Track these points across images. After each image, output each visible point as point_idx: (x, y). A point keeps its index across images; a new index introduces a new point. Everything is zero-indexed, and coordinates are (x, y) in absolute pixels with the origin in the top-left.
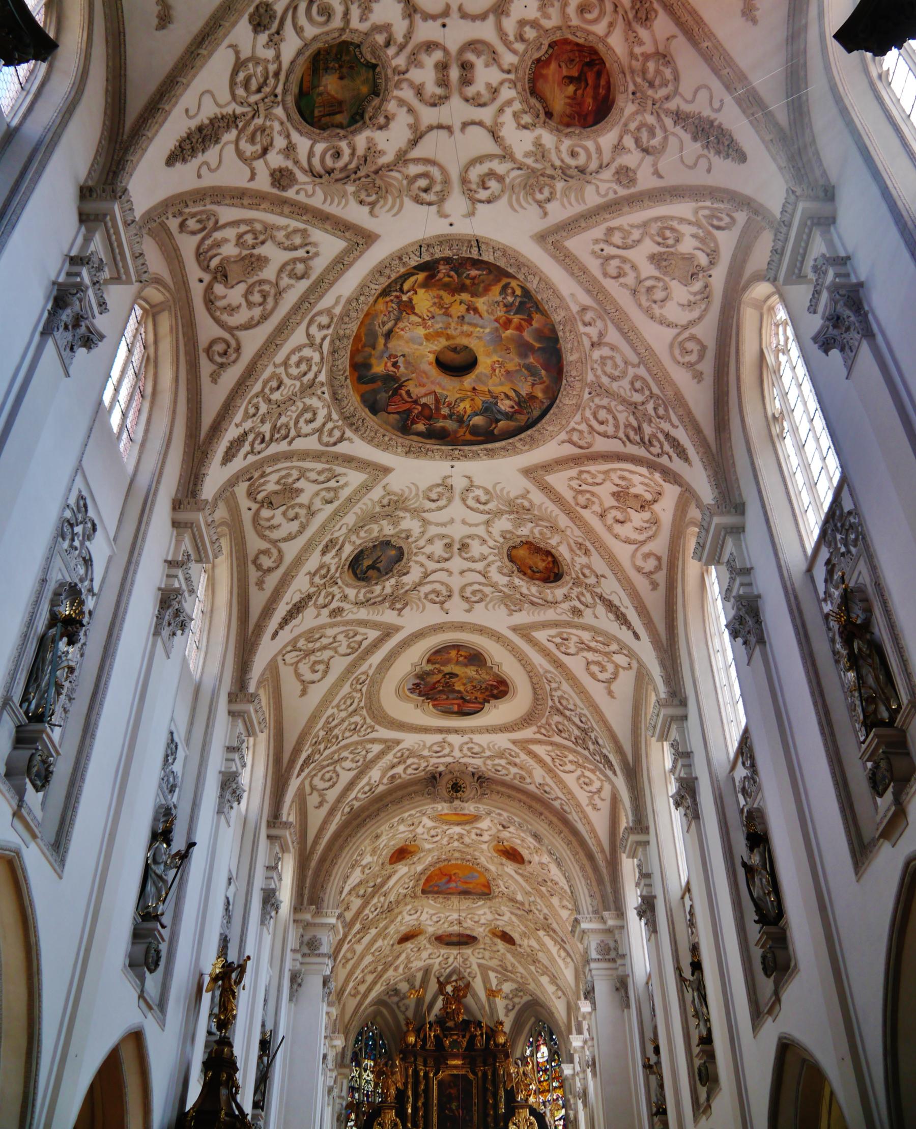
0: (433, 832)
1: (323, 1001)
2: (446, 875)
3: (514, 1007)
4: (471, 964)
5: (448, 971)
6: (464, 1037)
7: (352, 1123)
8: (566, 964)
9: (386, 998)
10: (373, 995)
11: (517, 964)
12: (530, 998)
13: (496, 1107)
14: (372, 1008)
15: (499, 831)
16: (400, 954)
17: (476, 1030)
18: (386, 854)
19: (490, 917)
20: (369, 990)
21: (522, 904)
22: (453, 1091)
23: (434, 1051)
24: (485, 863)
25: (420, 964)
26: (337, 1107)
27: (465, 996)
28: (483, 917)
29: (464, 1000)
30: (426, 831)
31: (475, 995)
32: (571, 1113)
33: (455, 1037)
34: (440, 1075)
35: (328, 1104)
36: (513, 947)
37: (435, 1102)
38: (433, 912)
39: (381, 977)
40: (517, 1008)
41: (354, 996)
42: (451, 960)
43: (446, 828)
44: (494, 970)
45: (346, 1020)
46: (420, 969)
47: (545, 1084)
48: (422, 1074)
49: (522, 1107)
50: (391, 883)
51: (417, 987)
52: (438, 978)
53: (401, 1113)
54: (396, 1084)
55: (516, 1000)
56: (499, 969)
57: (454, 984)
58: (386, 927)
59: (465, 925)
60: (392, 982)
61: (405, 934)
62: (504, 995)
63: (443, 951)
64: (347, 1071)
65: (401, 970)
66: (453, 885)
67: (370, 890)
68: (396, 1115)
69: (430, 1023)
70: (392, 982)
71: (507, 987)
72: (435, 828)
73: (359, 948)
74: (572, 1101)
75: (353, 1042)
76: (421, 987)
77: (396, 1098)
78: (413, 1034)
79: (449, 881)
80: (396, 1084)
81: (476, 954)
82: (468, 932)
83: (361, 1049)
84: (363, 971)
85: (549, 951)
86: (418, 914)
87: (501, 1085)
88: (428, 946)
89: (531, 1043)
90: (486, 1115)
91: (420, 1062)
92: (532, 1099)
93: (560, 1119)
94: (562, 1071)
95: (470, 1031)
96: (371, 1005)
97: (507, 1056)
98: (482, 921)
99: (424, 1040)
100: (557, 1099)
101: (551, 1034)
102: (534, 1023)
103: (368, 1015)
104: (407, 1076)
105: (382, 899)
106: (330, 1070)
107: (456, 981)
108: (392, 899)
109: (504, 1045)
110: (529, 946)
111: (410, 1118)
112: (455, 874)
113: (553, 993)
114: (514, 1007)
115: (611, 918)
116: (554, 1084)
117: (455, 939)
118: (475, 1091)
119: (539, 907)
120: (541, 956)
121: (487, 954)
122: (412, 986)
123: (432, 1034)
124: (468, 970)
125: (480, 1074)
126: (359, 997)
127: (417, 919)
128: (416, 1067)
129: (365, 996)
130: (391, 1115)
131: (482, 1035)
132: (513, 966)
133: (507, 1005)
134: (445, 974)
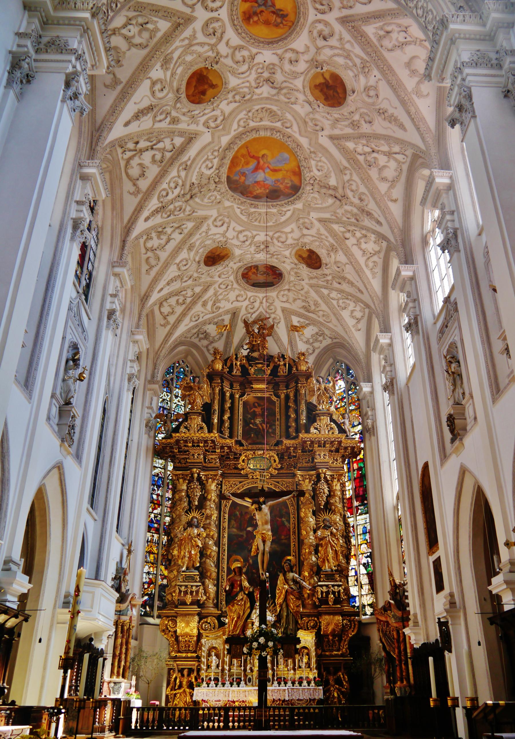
0: (238, 56)
2: (253, 157)
3: (314, 351)
4: (276, 308)
5: (254, 316)
6: (268, 366)
8: (374, 274)
9: (196, 341)
11: (320, 301)
12: (328, 341)
14: (183, 347)
15: (318, 49)
16: (208, 287)
17: (279, 361)
18: (182, 75)
19: (297, 234)
21: (335, 189)
22: (258, 410)
23: (240, 376)
24: (297, 135)
26: (146, 416)
28: (290, 236)
29: (267, 338)
30: (230, 51)
31: (278, 340)
32: (370, 422)
33: (260, 366)
34: (245, 398)
35: (128, 390)
36: (319, 272)
37: (241, 417)
38: (241, 228)
40: (317, 352)
41: (164, 326)
42: (257, 305)
43: (254, 51)
45: (157, 347)
46: (227, 312)
47: (341, 409)
48: (228, 394)
49: (324, 414)
50: (192, 152)
53: (207, 420)
54: (202, 397)
55: (316, 345)
56: (302, 311)
58: (191, 234)
59: (272, 249)
60: (201, 320)
61: (211, 252)
62: (305, 340)
63: (250, 294)
66: (260, 176)
67: (168, 155)
68: (203, 420)
71: (309, 332)
72: (240, 48)
73: (164, 255)
74: (370, 413)
75: (164, 370)
78: (220, 362)
79: (257, 169)
80: (202, 397)
81: (280, 297)
82: (274, 262)
83: (172, 379)
85: (357, 261)
86: (225, 225)
87: (303, 402)
88: (235, 285)
90: (288, 427)
91: (226, 384)
94: (361, 389)
95: (274, 362)
98: (290, 241)
99: (231, 368)
101: (348, 369)
102: (332, 364)
105: (183, 174)
106: (131, 361)
108: (194, 180)
110: (335, 262)
111: (216, 427)
112: (263, 156)
113: (354, 326)
114: (314, 351)
115: (497, 11)
116: (351, 408)
117: (261, 278)
118: (277, 410)
119: (354, 187)
120: (349, 273)
121: (291, 295)
123: (238, 363)
124: (273, 316)
125: (283, 396)
126: (168, 327)
127: (224, 235)
129: (175, 326)
130: (198, 420)
131: (285, 365)
132: (316, 304)
133: (307, 349)
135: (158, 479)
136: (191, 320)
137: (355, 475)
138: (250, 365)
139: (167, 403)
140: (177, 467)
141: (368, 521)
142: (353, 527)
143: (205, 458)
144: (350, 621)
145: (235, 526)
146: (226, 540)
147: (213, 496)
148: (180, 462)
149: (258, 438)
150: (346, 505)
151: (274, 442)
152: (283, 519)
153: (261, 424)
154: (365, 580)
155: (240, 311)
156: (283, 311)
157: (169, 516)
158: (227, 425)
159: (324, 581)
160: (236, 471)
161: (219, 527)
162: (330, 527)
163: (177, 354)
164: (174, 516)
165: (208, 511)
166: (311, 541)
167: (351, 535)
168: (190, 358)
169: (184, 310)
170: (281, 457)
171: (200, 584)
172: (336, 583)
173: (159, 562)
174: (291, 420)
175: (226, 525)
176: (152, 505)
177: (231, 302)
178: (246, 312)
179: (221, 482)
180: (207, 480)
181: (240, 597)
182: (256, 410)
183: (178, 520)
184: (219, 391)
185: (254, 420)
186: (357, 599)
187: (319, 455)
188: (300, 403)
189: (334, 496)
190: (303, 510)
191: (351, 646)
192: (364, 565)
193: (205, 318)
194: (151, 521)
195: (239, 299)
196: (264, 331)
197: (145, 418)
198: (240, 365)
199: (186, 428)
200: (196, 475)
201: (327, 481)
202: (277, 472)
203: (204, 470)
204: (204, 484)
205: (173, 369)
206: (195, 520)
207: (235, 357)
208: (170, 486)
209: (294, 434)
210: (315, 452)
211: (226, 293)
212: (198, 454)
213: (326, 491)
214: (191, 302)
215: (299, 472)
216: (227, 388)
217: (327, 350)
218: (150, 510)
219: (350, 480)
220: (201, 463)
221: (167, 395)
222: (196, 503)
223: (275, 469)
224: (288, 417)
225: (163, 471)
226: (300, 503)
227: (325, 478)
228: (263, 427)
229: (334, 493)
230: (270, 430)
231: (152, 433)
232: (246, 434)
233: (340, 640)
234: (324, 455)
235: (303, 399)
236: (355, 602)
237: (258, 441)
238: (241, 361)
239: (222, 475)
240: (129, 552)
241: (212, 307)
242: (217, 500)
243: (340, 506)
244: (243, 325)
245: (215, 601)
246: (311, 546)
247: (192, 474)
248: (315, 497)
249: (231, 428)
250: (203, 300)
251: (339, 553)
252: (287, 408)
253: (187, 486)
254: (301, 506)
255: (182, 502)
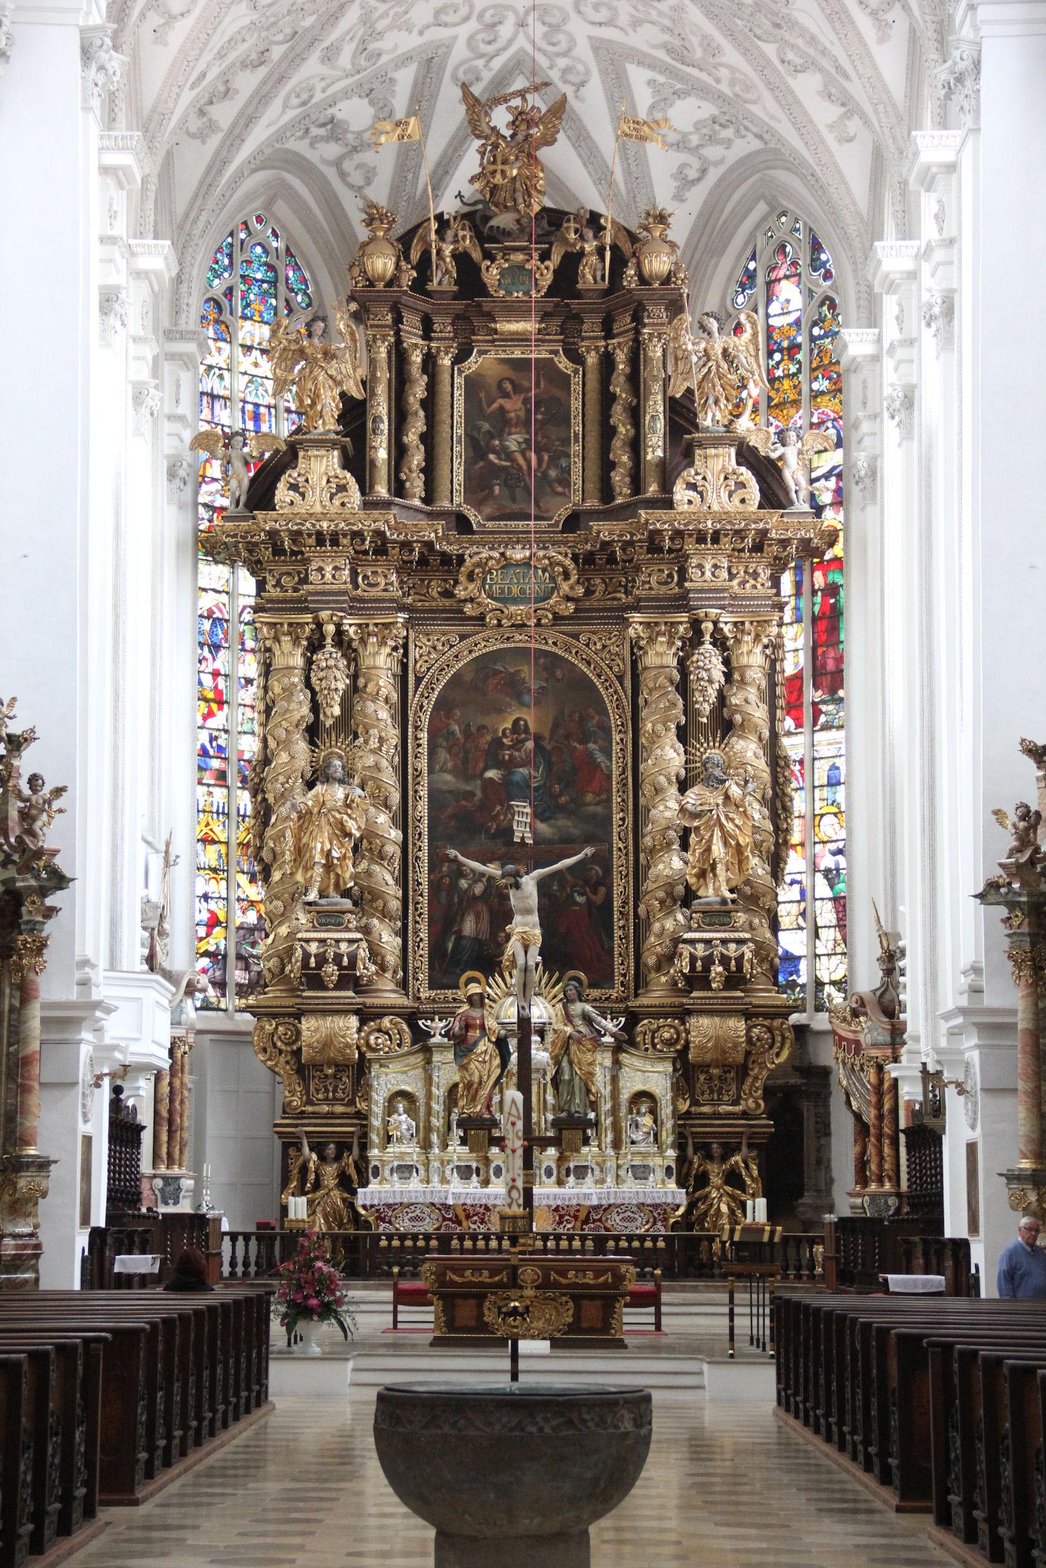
1: (87, 109)
5: (497, 63)
6: (545, 256)
7: (216, 486)
9: (301, 147)
10: (258, 136)
13: (636, 445)
14: (262, 176)
17: (582, 238)
20: (247, 119)
22: (513, 406)
23: (456, 297)
25: (408, 42)
26: (169, 446)
27: (549, 140)
29: (544, 154)
33: (520, 257)
34: (473, 363)
37: (459, 431)
39: (281, 79)
41: (201, 136)
42: (506, 30)
44: (643, 60)
45: (180, 207)
46: (407, 59)
48: (417, 358)
49: (717, 442)
51: (400, 114)
52: (465, 87)
54: (338, 383)
57: (516, 102)
60: (318, 96)
64: (191, 347)
65: (345, 60)
68: (347, 464)
69: (439, 217)
70: (318, 96)
76: (409, 115)
77: (339, 421)
78: (389, 250)
83: (229, 292)
84: (221, 55)
87: (657, 387)
89: (751, 276)
90: (608, 466)
92: (744, 424)
93: (827, 476)
95: (565, 241)
96: (261, 162)
97: (675, 307)
99: (424, 266)
100: (822, 423)
103: (251, 197)
104: (372, 363)
107: (522, 94)
109: (667, 280)
111: (382, 473)
118: (576, 404)
122: (383, 112)
123: (448, 249)
124: (562, 62)
125: (592, 359)
126: (215, 141)
128: (399, 342)
131: (600, 251)
134: (487, 76)
135: (214, 624)
136: (286, 106)
137: (817, 608)
138: (488, 256)
139: (221, 377)
140: (270, 601)
141: (843, 752)
142: (801, 762)
143: (354, 574)
144: (770, 1030)
145: (450, 765)
146: (423, 807)
147: (385, 683)
148: (278, 584)
149: (513, 499)
150: (781, 702)
151: (562, 513)
152: (591, 746)
153: (523, 452)
154: (826, 914)
155: (447, 55)
156: (595, 50)
157: (253, 733)
158: (417, 459)
159: (699, 929)
160: (447, 602)
161: (403, 771)
162: (724, 781)
163: (241, 207)
164: (272, 743)
165: (374, 743)
166: (668, 814)
167: (794, 785)
168: (281, 208)
169: (264, 83)
170: (586, 562)
171: (359, 936)
172: (733, 935)
173: (234, 868)
174: (617, 443)
175: (423, 764)
176: (202, 704)
177: (416, 29)
178: (468, 54)
179: (406, 638)
180: (363, 641)
181: (481, 1047)
182: (508, 404)
183: (284, 757)
184: (389, 352)
185: (501, 436)
186: (803, 966)
187: (700, 566)
188: (648, 393)
189: (743, 682)
190: (649, 726)
191: (769, 1092)
192: (827, 872)
193: (330, 91)
194: (204, 753)
195: (444, 18)
196: (534, 131)
197: (167, 451)
198: (455, 256)
199: (294, 487)
200: (330, 629)
201: (720, 642)
202: (571, 606)
203: (352, 611)
204: (355, 651)
205: (230, 256)
206: (338, 763)
207: (434, 226)
208: (250, 644)
209: (627, 491)
210: (687, 557)
211: (401, 10)
212: (336, 568)
213: (718, 674)
214: (285, 56)
215: (636, 617)
216: (413, 339)
217: (745, 166)
218: (200, 722)
219: (798, 620)
220: (345, 593)
221: (219, 350)
222: (337, 711)
223: (568, 599)
224: (608, 432)
225: (224, 598)
226: (641, 702)
227: (717, 629)
228: (529, 462)
229: (742, 676)
230: (553, 473)
231: (189, 489)
232: (477, 488)
233: (741, 1080)
234: (715, 566)
235: (655, 379)
236: (797, 972)
237: (515, 507)
238: (456, 241)
239: (407, 624)
240: (167, 864)
241: (354, 57)
242: (395, 697)
243: (759, 713)
244: (458, 93)
245: (401, 974)
246: (668, 828)
247: (319, 625)
248: (684, 688)
249: (429, 470)
250: (326, 44)
251: (748, 853)
252: (607, 399)
253: (303, 655)
254: (644, 714)
255: (293, 706)
